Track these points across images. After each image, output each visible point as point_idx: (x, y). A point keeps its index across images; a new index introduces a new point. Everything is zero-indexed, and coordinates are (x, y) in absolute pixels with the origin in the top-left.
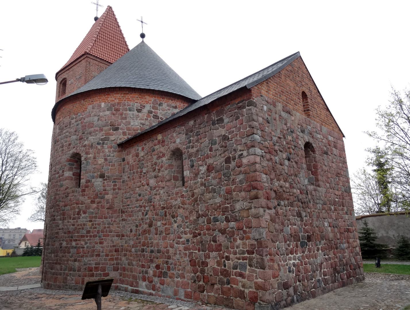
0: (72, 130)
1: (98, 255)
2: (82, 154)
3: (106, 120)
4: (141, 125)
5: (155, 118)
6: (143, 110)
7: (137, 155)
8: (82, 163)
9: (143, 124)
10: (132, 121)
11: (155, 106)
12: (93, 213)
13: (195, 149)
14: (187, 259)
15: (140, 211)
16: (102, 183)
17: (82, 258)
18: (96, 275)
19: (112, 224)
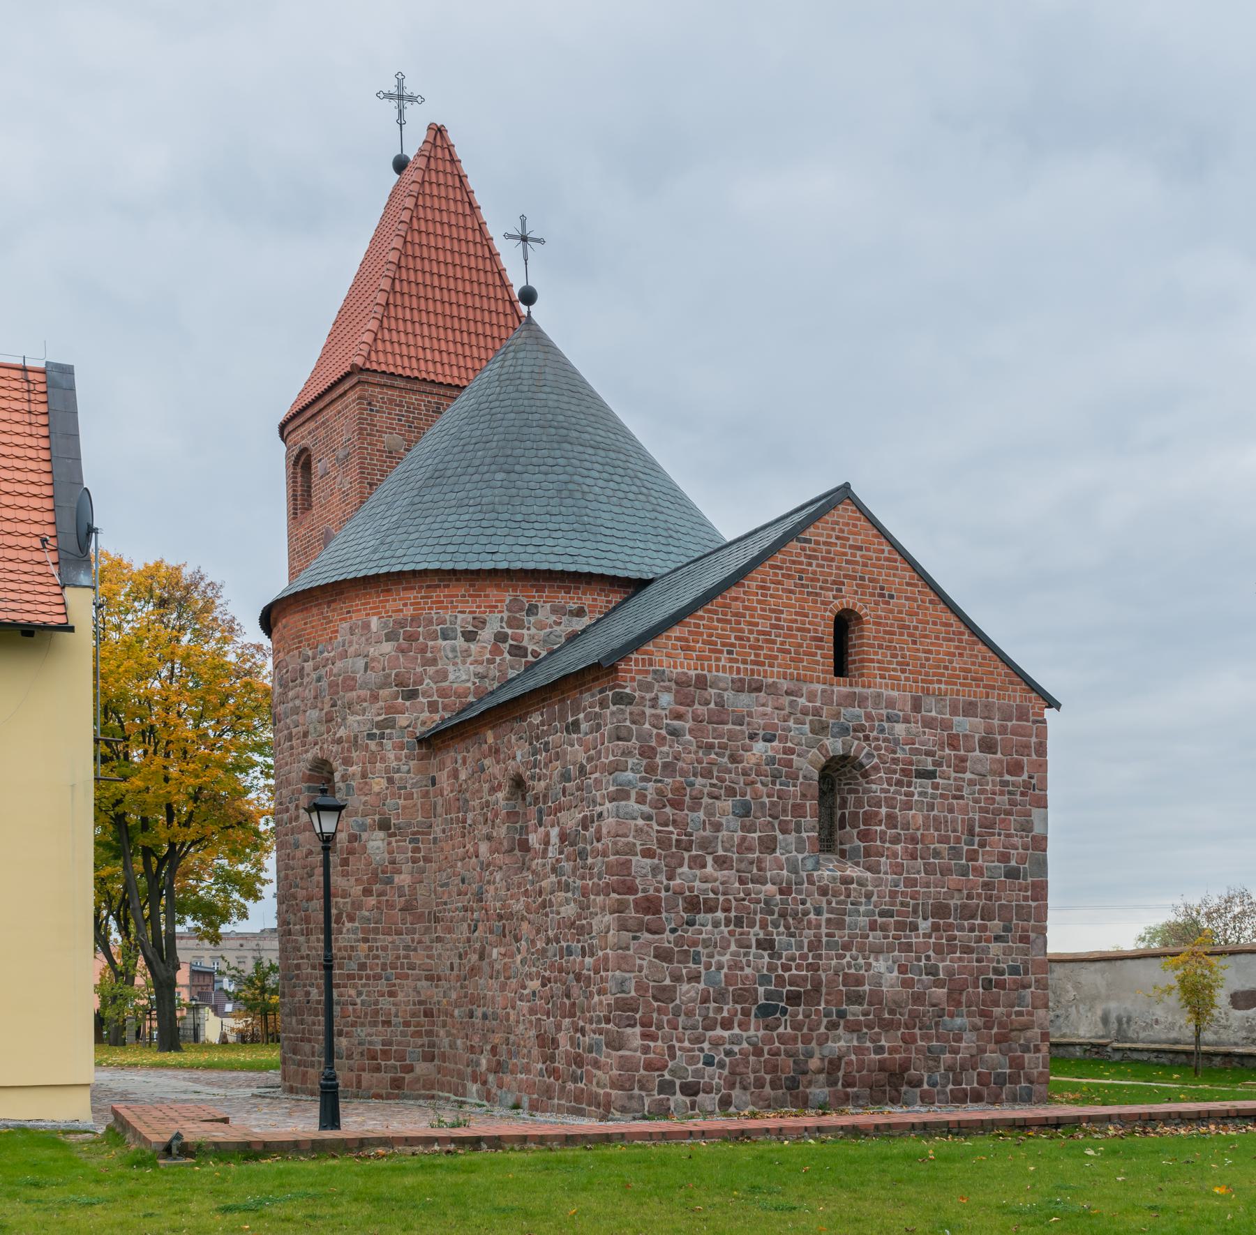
0: (309, 694)
1: (387, 1023)
2: (335, 764)
3: (384, 670)
4: (477, 681)
5: (516, 655)
6: (480, 632)
7: (455, 773)
8: (337, 789)
9: (482, 677)
10: (451, 668)
11: (514, 617)
12: (369, 920)
14: (533, 1033)
15: (464, 919)
16: (386, 842)
17: (354, 1029)
18: (386, 1068)
19: (415, 950)
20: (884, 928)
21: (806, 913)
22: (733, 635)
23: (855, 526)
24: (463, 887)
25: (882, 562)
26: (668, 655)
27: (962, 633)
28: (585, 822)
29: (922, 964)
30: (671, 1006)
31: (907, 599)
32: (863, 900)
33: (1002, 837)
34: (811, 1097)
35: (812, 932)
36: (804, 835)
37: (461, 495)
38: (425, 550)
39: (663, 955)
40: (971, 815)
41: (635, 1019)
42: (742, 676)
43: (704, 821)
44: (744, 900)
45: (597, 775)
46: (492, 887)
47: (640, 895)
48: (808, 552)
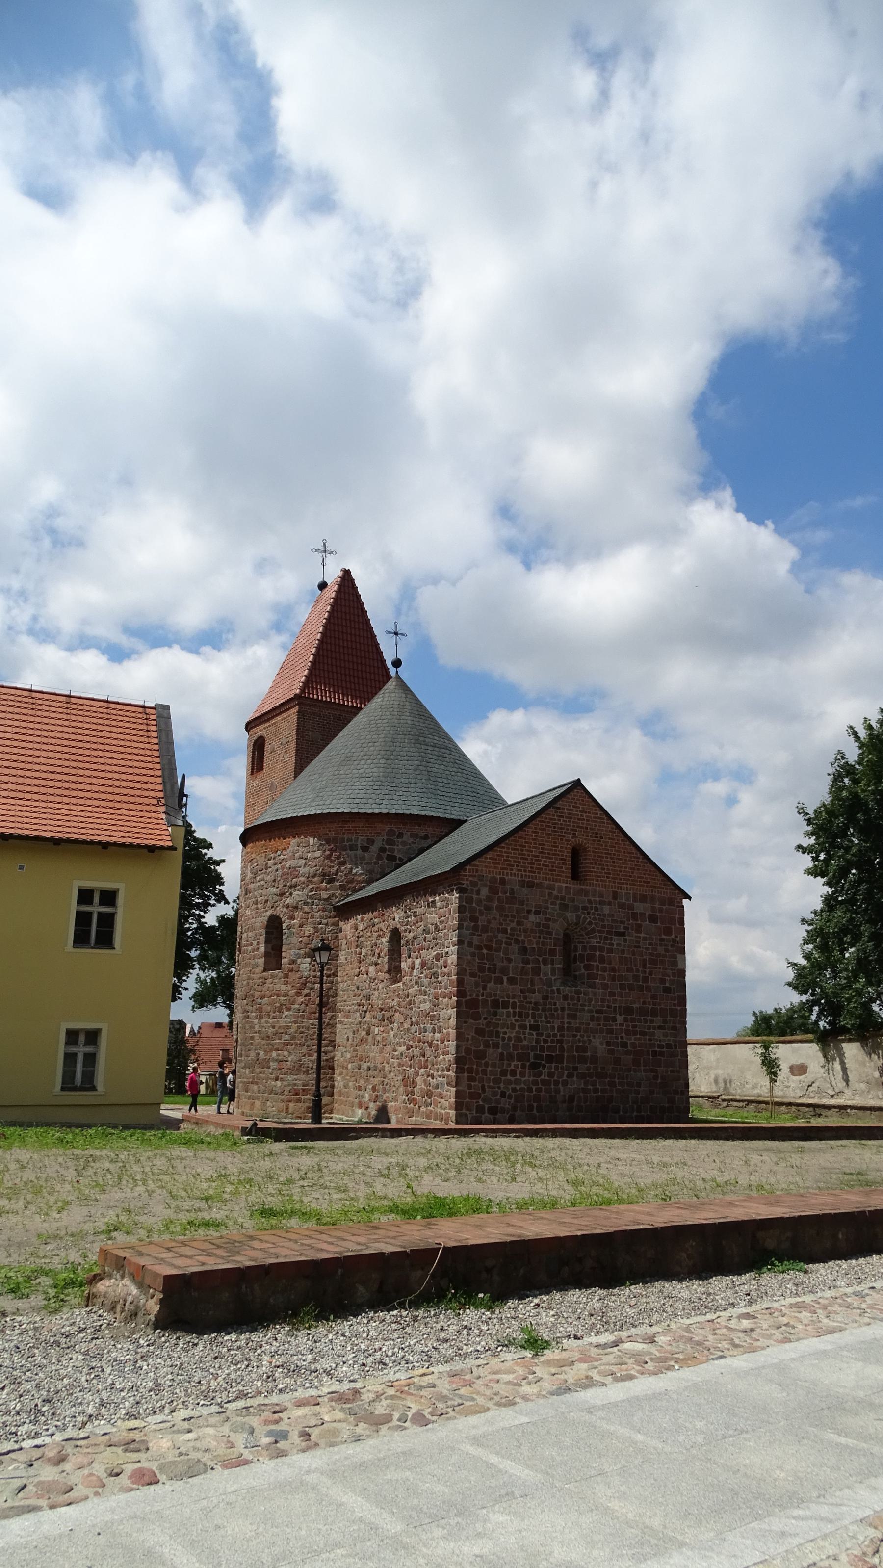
0: (269, 878)
13: (412, 934)
20: (598, 1019)
24: (358, 992)
26: (486, 867)
28: (438, 957)
37: (361, 771)
38: (342, 801)
45: (446, 931)
46: (376, 992)
47: (468, 998)
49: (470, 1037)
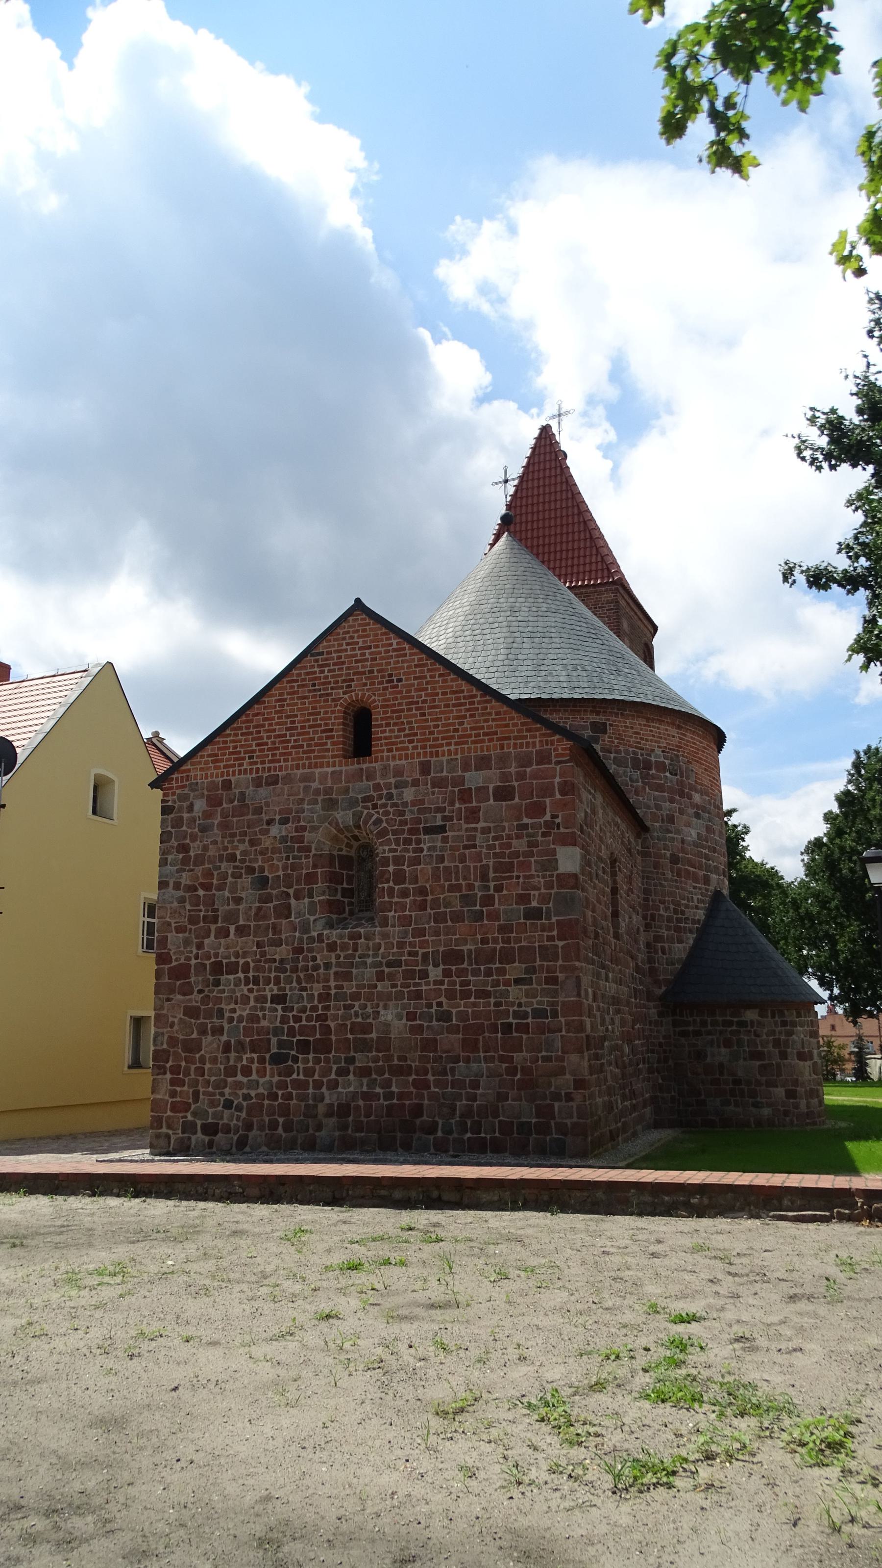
20: (391, 977)
21: (316, 968)
22: (254, 743)
23: (364, 630)
25: (391, 653)
26: (202, 769)
27: (475, 696)
29: (433, 1010)
30: (197, 1056)
31: (415, 678)
32: (371, 953)
33: (521, 880)
34: (318, 1141)
35: (321, 985)
36: (316, 899)
39: (191, 1012)
40: (484, 862)
41: (164, 1067)
42: (260, 774)
43: (228, 898)
44: (260, 961)
47: (174, 964)
48: (320, 663)
49: (176, 1020)
